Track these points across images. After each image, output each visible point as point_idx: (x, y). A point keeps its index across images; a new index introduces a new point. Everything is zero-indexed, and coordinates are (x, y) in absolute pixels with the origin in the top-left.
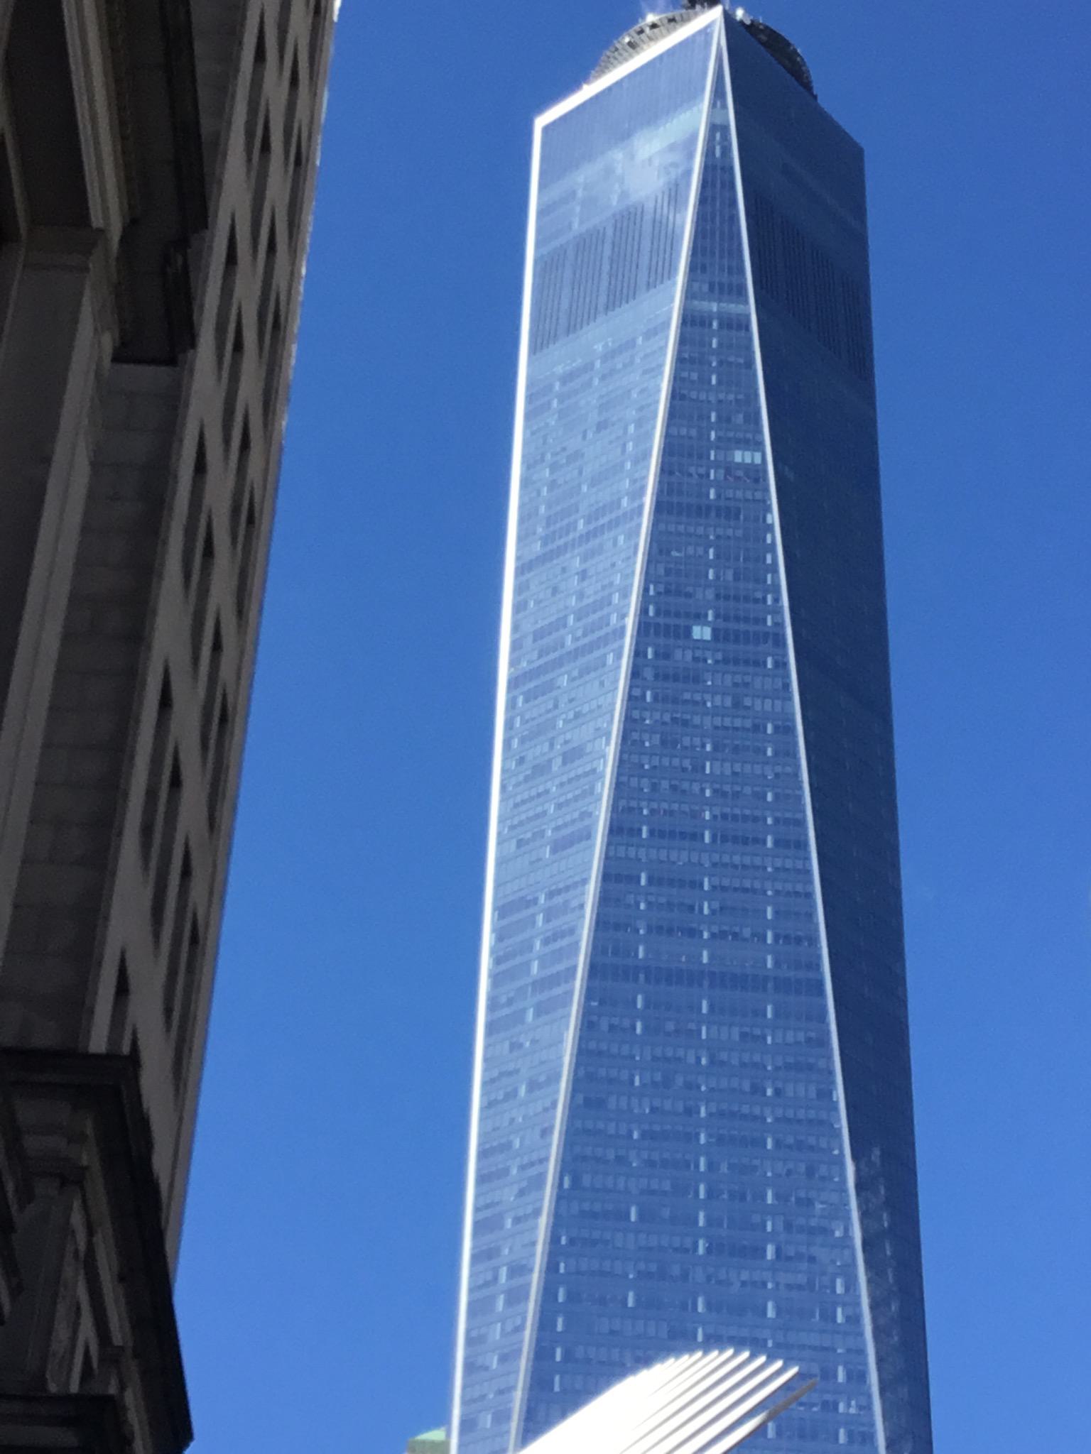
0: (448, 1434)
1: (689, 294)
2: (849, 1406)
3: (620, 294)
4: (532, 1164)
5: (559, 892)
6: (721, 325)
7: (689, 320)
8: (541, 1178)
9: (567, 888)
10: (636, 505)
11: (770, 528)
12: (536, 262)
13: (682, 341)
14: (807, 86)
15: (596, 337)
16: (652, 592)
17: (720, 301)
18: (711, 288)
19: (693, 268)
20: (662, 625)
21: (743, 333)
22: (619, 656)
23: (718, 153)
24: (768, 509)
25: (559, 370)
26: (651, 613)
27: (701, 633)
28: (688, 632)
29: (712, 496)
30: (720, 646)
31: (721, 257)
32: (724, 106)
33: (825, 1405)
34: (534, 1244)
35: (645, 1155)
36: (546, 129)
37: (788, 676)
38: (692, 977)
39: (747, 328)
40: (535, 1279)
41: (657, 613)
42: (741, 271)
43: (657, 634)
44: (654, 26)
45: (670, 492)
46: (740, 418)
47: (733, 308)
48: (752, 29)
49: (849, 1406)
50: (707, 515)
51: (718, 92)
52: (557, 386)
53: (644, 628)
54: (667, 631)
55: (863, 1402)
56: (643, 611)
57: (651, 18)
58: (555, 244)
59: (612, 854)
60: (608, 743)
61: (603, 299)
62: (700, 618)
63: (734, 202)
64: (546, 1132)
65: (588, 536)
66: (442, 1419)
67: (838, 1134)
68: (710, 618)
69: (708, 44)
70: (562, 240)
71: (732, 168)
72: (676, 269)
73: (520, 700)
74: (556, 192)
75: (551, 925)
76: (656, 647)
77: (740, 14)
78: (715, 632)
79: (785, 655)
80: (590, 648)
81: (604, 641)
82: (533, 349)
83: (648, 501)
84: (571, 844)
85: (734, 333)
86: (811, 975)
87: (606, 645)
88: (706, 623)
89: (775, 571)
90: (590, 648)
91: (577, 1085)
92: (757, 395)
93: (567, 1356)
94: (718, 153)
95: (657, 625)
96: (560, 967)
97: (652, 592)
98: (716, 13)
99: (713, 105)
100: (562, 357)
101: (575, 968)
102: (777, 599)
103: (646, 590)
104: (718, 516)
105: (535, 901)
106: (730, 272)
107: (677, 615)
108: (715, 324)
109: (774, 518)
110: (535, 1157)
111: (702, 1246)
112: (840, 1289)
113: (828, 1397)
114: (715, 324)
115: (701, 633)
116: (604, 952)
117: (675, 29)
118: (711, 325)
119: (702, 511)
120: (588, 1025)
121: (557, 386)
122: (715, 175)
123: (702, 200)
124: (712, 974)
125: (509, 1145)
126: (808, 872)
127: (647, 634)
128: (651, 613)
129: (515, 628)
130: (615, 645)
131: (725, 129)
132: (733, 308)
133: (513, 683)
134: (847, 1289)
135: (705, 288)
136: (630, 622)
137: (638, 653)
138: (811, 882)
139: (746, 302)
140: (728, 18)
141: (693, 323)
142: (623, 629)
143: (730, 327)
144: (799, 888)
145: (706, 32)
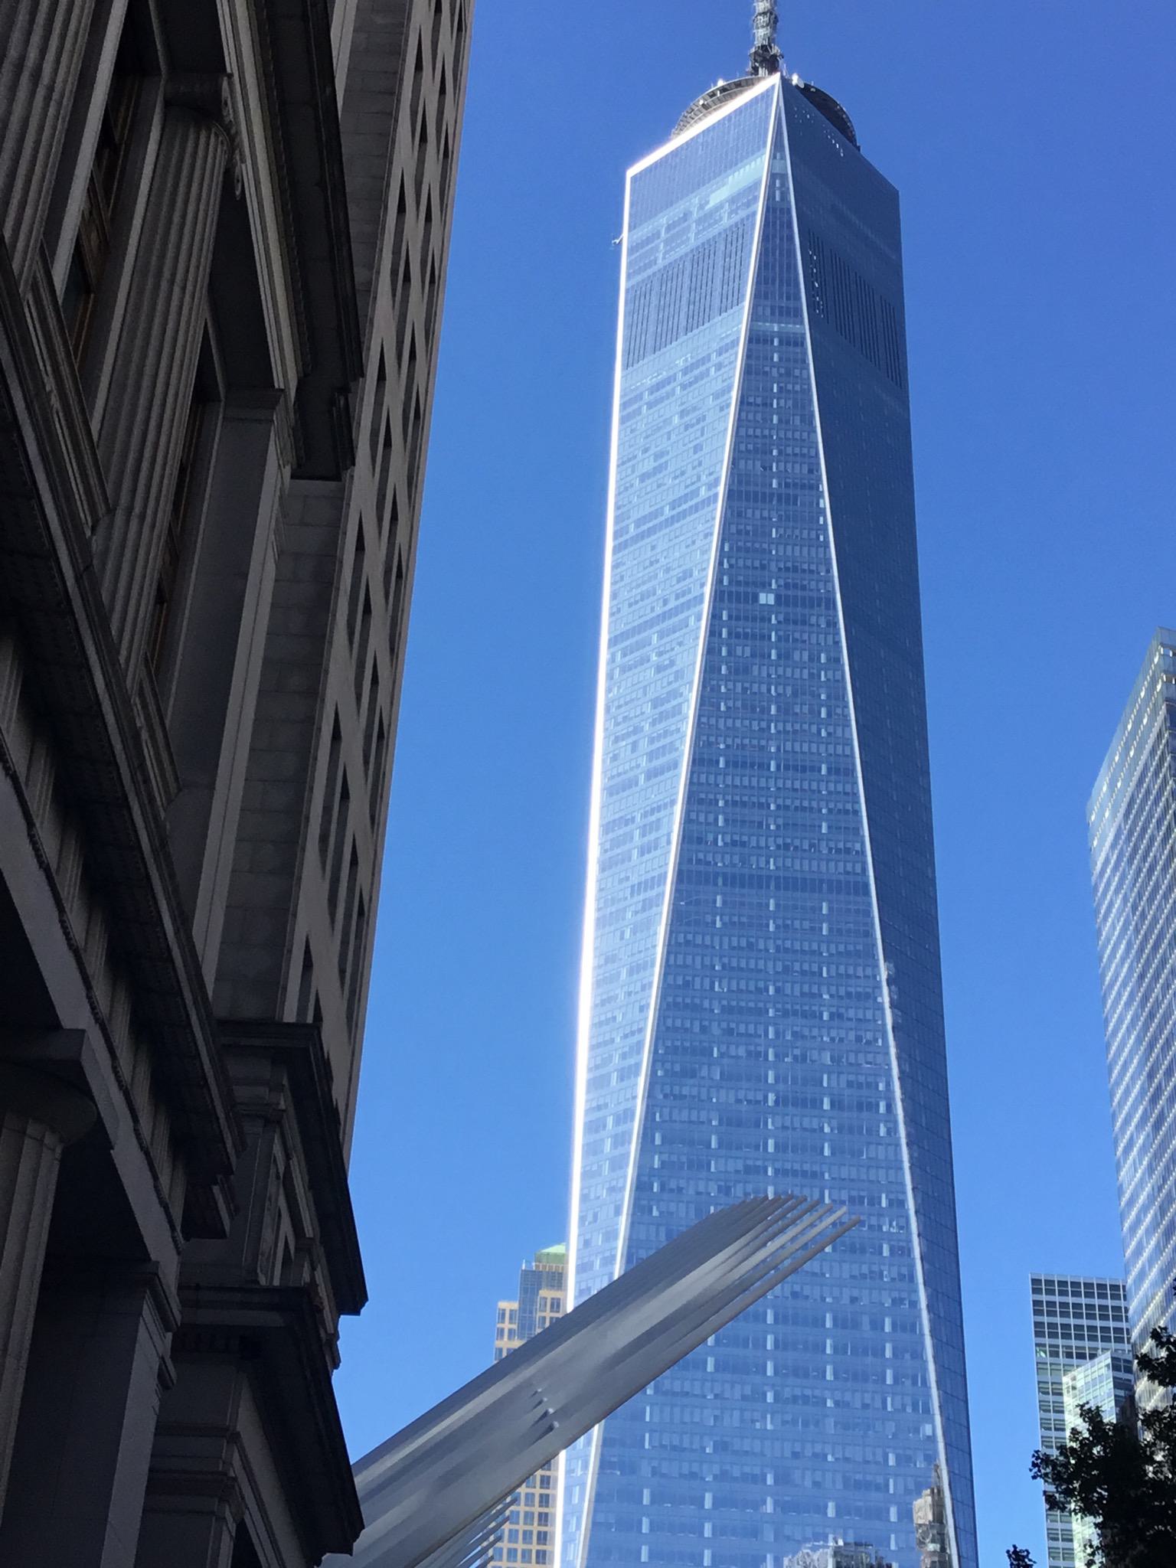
0: (567, 1249)
1: (754, 316)
3: (698, 317)
4: (633, 1033)
5: (652, 812)
6: (781, 342)
7: (756, 340)
8: (640, 1045)
9: (659, 809)
10: (711, 493)
11: (823, 512)
12: (627, 291)
13: (749, 355)
14: (852, 139)
15: (678, 355)
16: (726, 565)
17: (779, 323)
18: (773, 313)
19: (757, 296)
20: (733, 595)
21: (798, 350)
22: (699, 619)
23: (778, 199)
24: (821, 495)
25: (649, 382)
26: (725, 583)
27: (766, 598)
28: (756, 598)
29: (774, 485)
30: (782, 609)
32: (783, 158)
34: (635, 1098)
35: (724, 1025)
36: (634, 179)
37: (838, 633)
38: (759, 881)
39: (803, 344)
40: (636, 1126)
41: (730, 582)
42: (798, 298)
43: (730, 600)
44: (723, 90)
45: (740, 482)
46: (798, 421)
47: (791, 328)
48: (806, 90)
49: (891, 1225)
50: (771, 501)
51: (777, 145)
52: (646, 395)
53: (719, 596)
56: (718, 581)
57: (721, 83)
58: (645, 275)
60: (690, 691)
61: (683, 323)
62: (765, 586)
63: (791, 238)
64: (643, 1009)
65: (673, 520)
66: (562, 1237)
68: (774, 586)
69: (768, 106)
70: (650, 272)
72: (744, 296)
73: (619, 654)
74: (645, 230)
75: (646, 839)
76: (729, 610)
77: (795, 80)
78: (778, 598)
79: (836, 616)
80: (676, 611)
81: (687, 605)
82: (626, 366)
83: (721, 489)
84: (662, 773)
85: (791, 349)
86: (859, 879)
87: (689, 608)
88: (771, 591)
90: (676, 611)
91: (668, 969)
92: (811, 401)
93: (662, 1187)
94: (778, 199)
95: (730, 593)
96: (655, 874)
97: (726, 565)
98: (775, 79)
99: (773, 157)
100: (649, 372)
101: (666, 873)
102: (829, 571)
103: (721, 563)
104: (779, 500)
105: (633, 819)
106: (788, 298)
107: (747, 584)
108: (776, 343)
109: (826, 503)
110: (635, 1028)
111: (771, 1097)
112: (883, 1131)
114: (776, 343)
115: (766, 598)
116: (690, 861)
117: (741, 92)
118: (772, 342)
119: (765, 497)
120: (678, 918)
121: (646, 395)
122: (775, 213)
123: (765, 238)
124: (777, 878)
125: (614, 1018)
126: (856, 795)
127: (722, 600)
128: (725, 583)
129: (614, 596)
130: (696, 610)
131: (784, 177)
132: (791, 328)
133: (613, 642)
134: (889, 1132)
135: (768, 311)
136: (707, 590)
137: (715, 616)
138: (858, 802)
139: (802, 323)
140: (785, 83)
141: (758, 341)
142: (702, 595)
143: (788, 344)
144: (849, 807)
145: (767, 95)
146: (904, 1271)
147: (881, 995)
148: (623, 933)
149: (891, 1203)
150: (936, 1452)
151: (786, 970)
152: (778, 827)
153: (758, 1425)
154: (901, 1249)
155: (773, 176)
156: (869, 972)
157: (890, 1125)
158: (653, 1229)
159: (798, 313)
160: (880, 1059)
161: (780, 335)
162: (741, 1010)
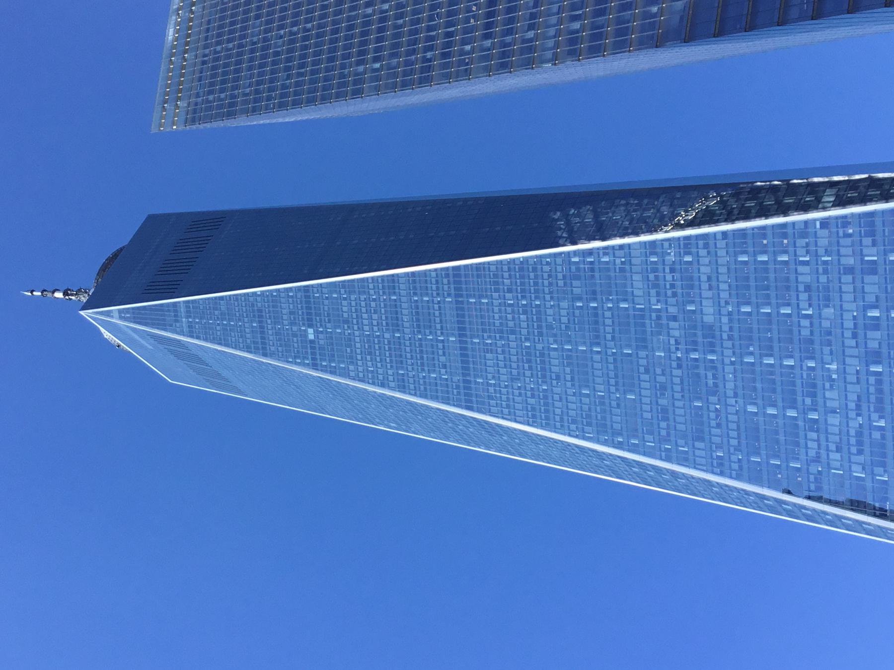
1: (182, 333)
2: (669, 254)
6: (190, 317)
8: (577, 446)
18: (176, 321)
28: (312, 342)
31: (164, 315)
33: (672, 270)
35: (554, 382)
39: (188, 302)
41: (308, 359)
42: (168, 305)
51: (108, 314)
53: (315, 367)
54: (313, 354)
55: (666, 244)
59: (413, 392)
63: (144, 307)
67: (526, 259)
71: (133, 308)
78: (310, 326)
86: (451, 272)
89: (278, 290)
99: (112, 317)
113: (667, 270)
122: (137, 317)
131: (120, 311)
132: (183, 309)
134: (605, 254)
135: (178, 325)
139: (179, 302)
146: (701, 243)
147: (519, 259)
148: (519, 445)
149: (653, 253)
150: (837, 218)
151: (513, 332)
152: (431, 333)
153: (834, 376)
154: (686, 245)
155: (121, 318)
156: (505, 268)
157: (601, 252)
158: (697, 452)
159: (175, 304)
160: (559, 261)
161: (188, 317)
162: (543, 369)
